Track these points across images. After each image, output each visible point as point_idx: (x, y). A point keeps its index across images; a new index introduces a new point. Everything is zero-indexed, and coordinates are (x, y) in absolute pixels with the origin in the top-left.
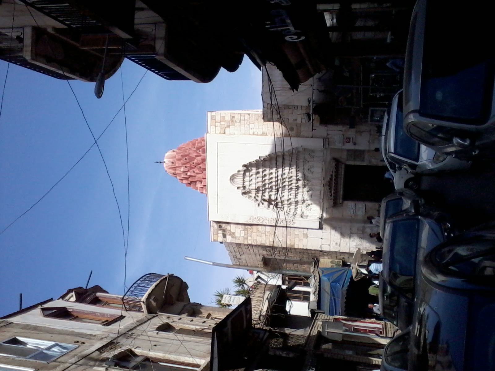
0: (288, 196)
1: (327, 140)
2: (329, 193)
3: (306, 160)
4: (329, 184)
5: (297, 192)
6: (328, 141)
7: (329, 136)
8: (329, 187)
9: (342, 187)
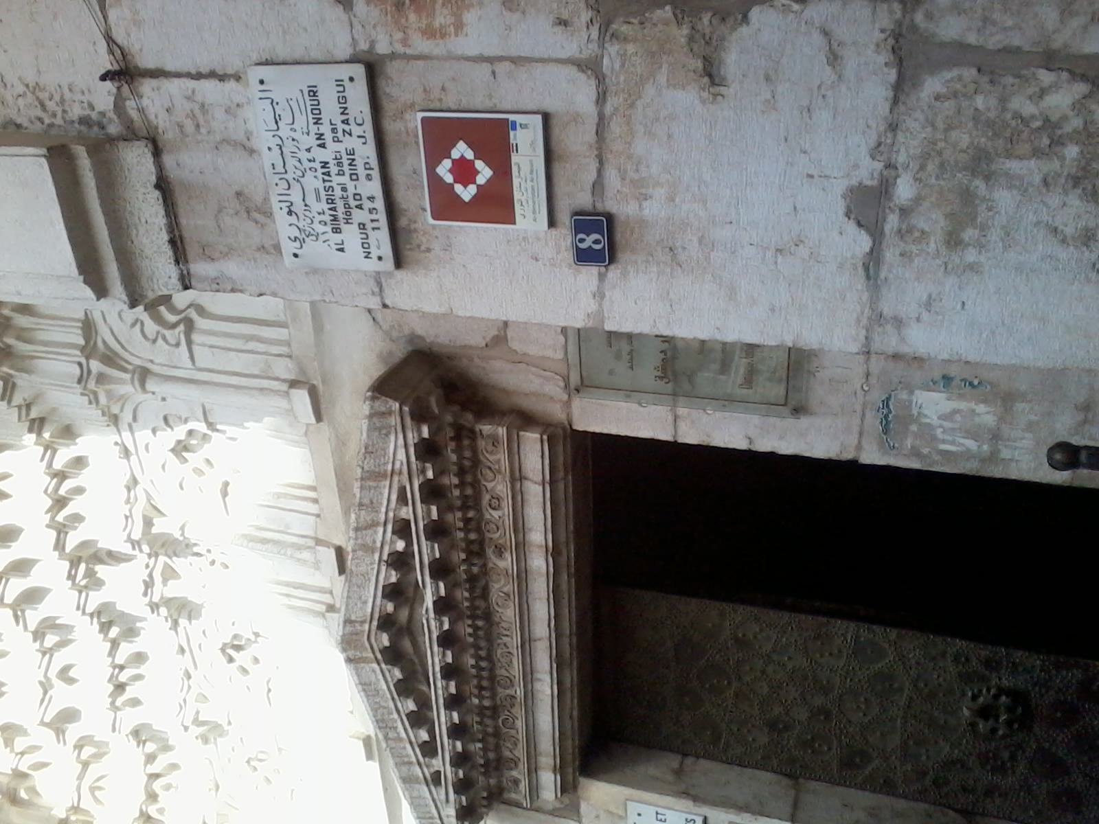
0: (46, 687)
1: (137, 163)
2: (401, 728)
3: (110, 359)
4: (385, 640)
5: (126, 650)
6: (163, 185)
7: (155, 101)
8: (398, 674)
9: (543, 660)
